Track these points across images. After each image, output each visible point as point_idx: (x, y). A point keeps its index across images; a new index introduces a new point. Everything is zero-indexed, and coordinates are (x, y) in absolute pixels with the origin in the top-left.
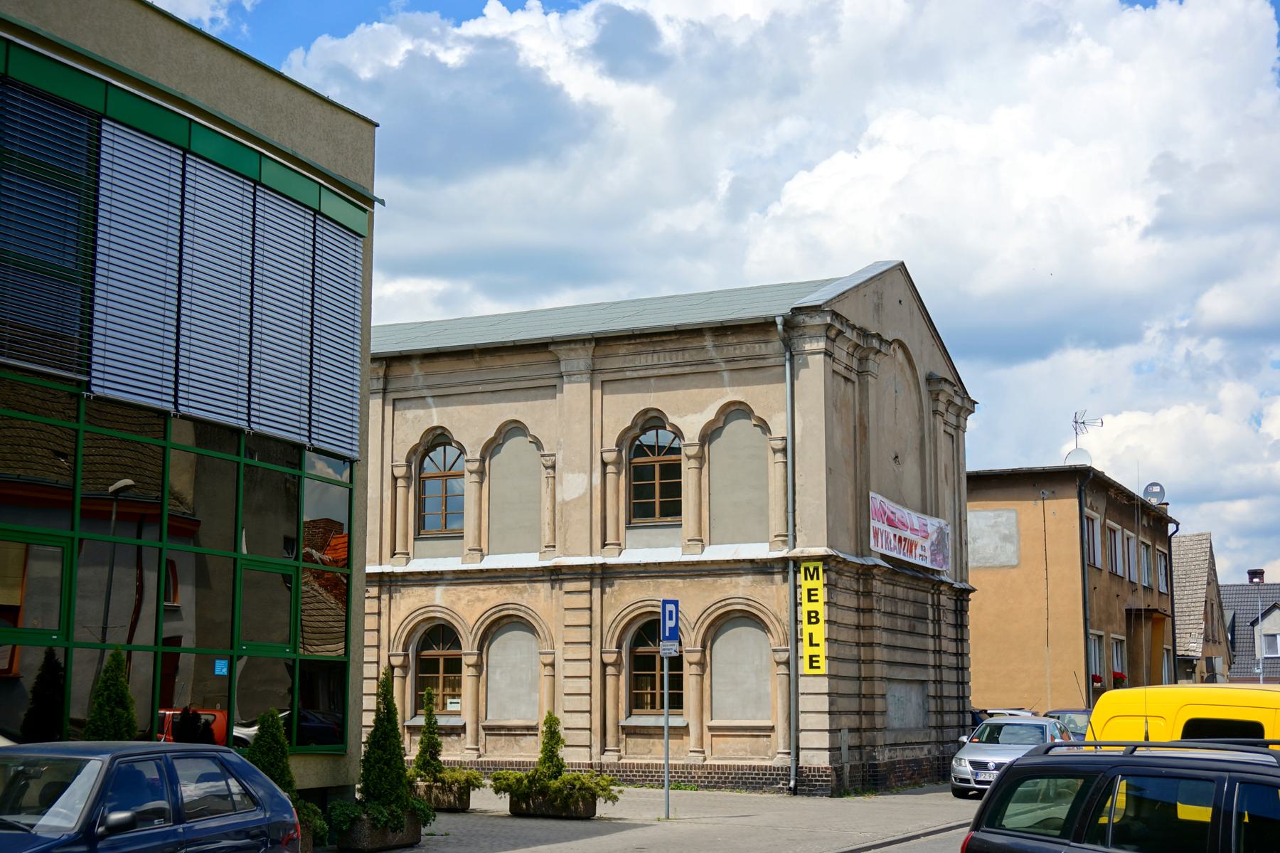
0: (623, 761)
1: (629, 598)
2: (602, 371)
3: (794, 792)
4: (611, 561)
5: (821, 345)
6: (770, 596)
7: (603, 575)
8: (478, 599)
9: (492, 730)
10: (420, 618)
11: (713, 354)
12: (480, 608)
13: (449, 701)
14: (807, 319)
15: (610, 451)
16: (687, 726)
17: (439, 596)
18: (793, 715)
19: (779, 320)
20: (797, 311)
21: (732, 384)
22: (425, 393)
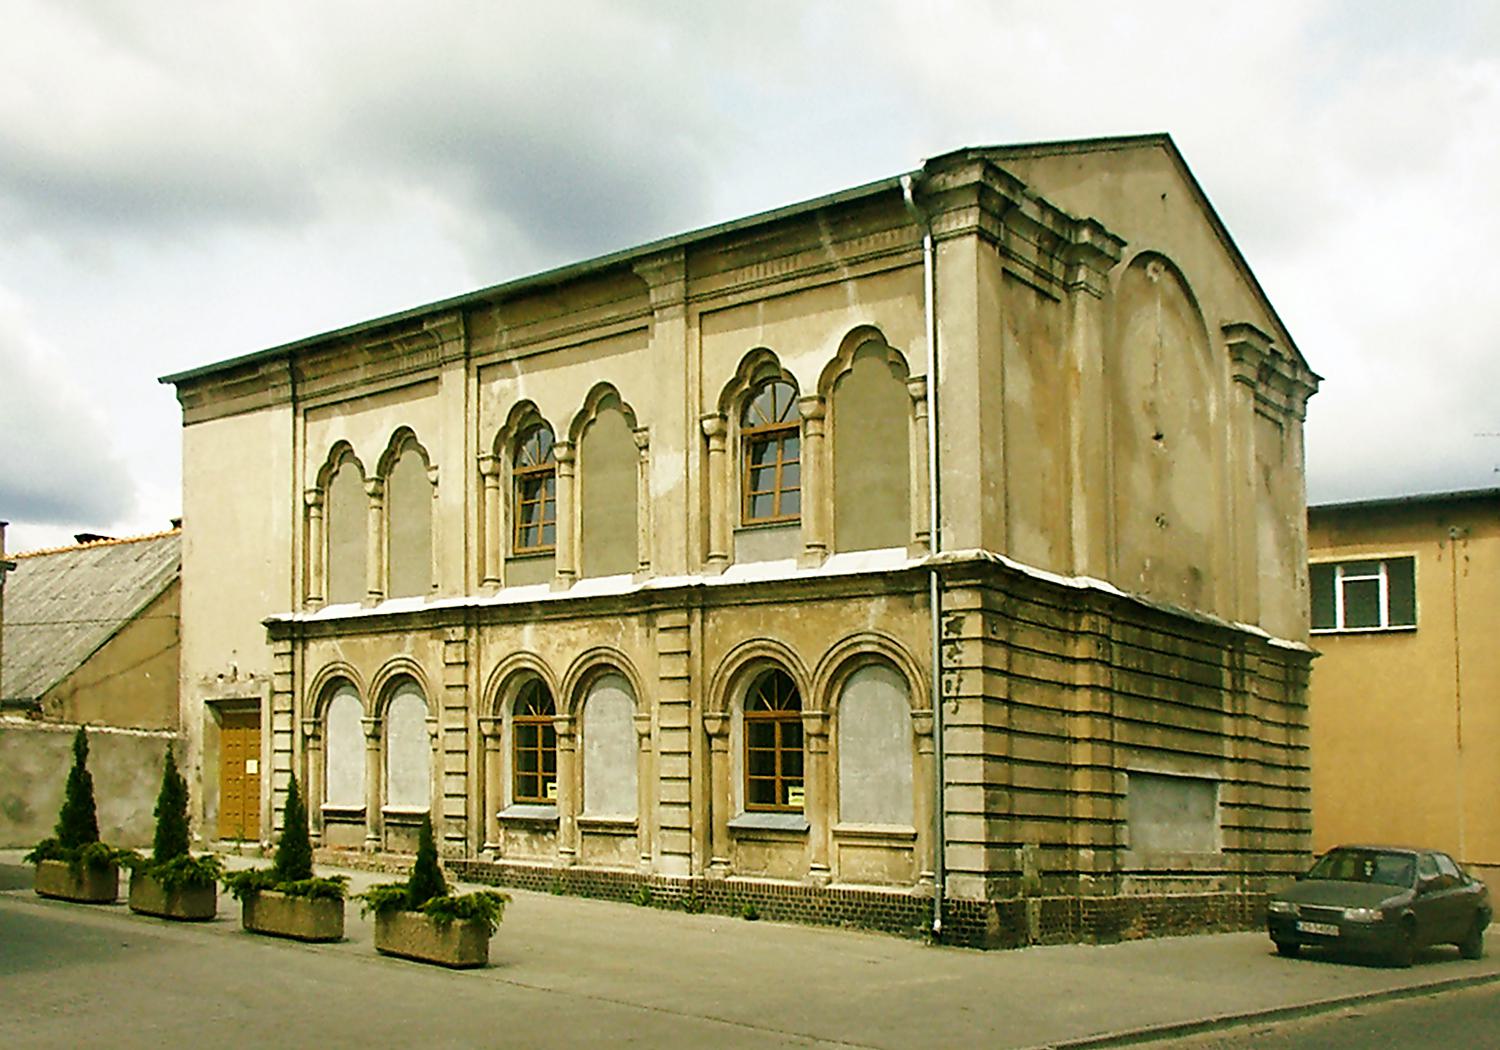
0: (500, 862)
1: (732, 634)
2: (700, 299)
3: (939, 939)
4: (712, 580)
5: (971, 220)
6: (915, 632)
7: (702, 599)
8: (569, 642)
9: (589, 829)
10: (509, 670)
11: (832, 255)
12: (571, 654)
13: (791, 790)
14: (949, 179)
15: (710, 417)
16: (557, 821)
17: (528, 637)
18: (940, 814)
19: (906, 183)
20: (935, 165)
21: (862, 299)
22: (511, 354)
